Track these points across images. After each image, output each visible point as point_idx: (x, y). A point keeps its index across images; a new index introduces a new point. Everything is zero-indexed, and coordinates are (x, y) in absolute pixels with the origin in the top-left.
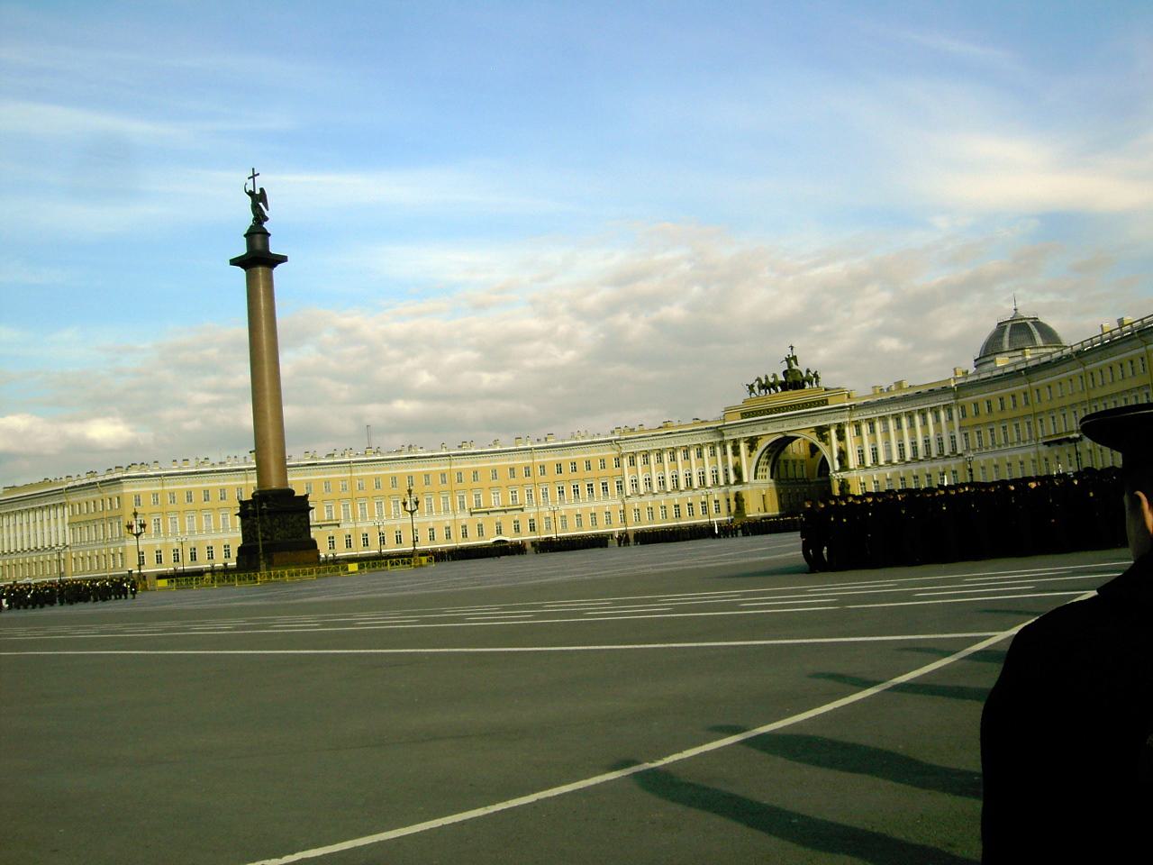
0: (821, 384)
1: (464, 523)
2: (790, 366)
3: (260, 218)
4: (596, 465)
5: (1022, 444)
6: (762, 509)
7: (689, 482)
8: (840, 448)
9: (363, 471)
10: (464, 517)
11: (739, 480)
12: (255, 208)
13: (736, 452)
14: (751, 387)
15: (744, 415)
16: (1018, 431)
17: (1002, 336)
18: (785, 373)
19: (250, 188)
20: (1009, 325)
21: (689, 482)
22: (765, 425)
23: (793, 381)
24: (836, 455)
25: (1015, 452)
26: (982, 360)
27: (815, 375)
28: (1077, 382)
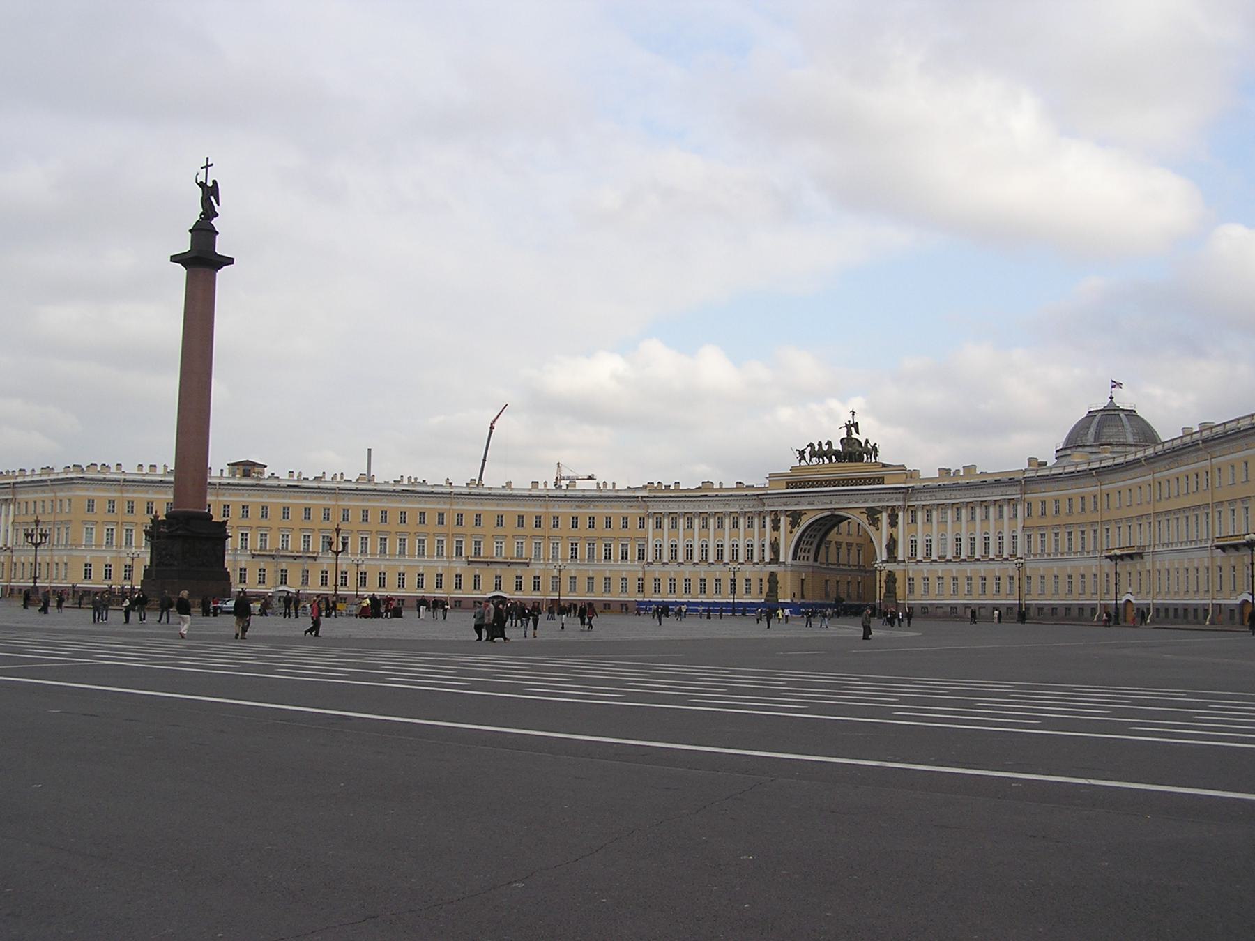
0: (879, 459)
1: (459, 572)
2: (849, 433)
3: (209, 212)
4: (617, 523)
5: (1086, 555)
6: (798, 595)
7: (720, 554)
9: (350, 500)
10: (459, 566)
11: (775, 560)
12: (206, 202)
13: (776, 527)
14: (802, 453)
15: (790, 484)
16: (1083, 539)
17: (1089, 428)
19: (201, 179)
20: (1099, 415)
21: (720, 554)
22: (811, 499)
23: (853, 450)
24: (884, 543)
25: (1076, 563)
26: (1063, 453)
27: (874, 447)
28: (1146, 489)
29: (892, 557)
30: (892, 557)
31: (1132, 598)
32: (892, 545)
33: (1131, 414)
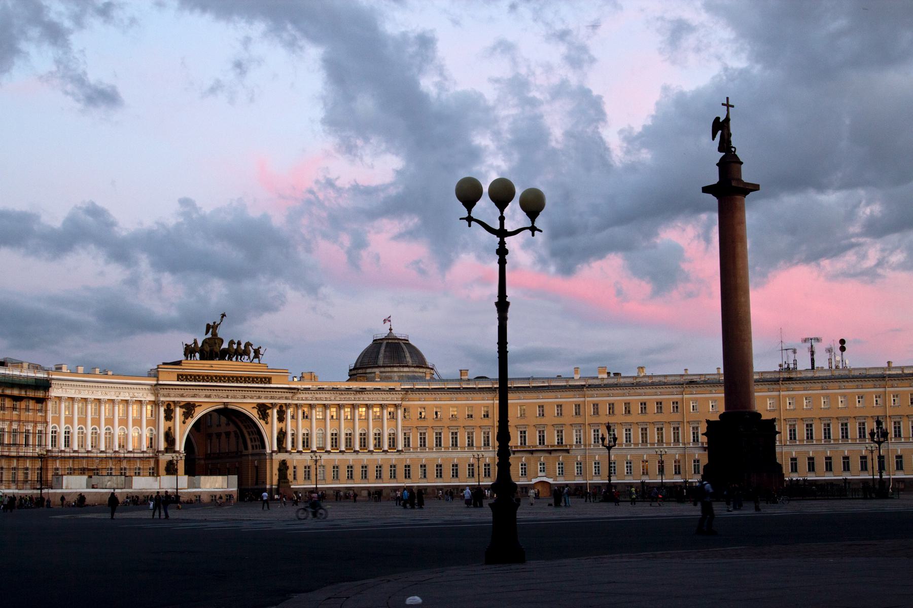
0: (263, 359)
2: (214, 334)
3: (725, 145)
8: (281, 429)
13: (169, 416)
17: (378, 353)
18: (204, 342)
22: (208, 393)
27: (257, 353)
29: (281, 448)
30: (281, 448)
31: (551, 481)
32: (282, 435)
33: (406, 342)
